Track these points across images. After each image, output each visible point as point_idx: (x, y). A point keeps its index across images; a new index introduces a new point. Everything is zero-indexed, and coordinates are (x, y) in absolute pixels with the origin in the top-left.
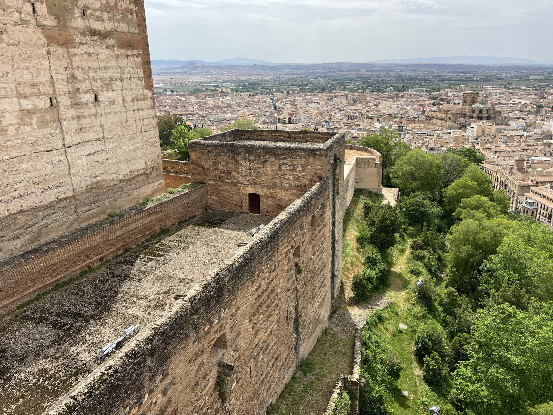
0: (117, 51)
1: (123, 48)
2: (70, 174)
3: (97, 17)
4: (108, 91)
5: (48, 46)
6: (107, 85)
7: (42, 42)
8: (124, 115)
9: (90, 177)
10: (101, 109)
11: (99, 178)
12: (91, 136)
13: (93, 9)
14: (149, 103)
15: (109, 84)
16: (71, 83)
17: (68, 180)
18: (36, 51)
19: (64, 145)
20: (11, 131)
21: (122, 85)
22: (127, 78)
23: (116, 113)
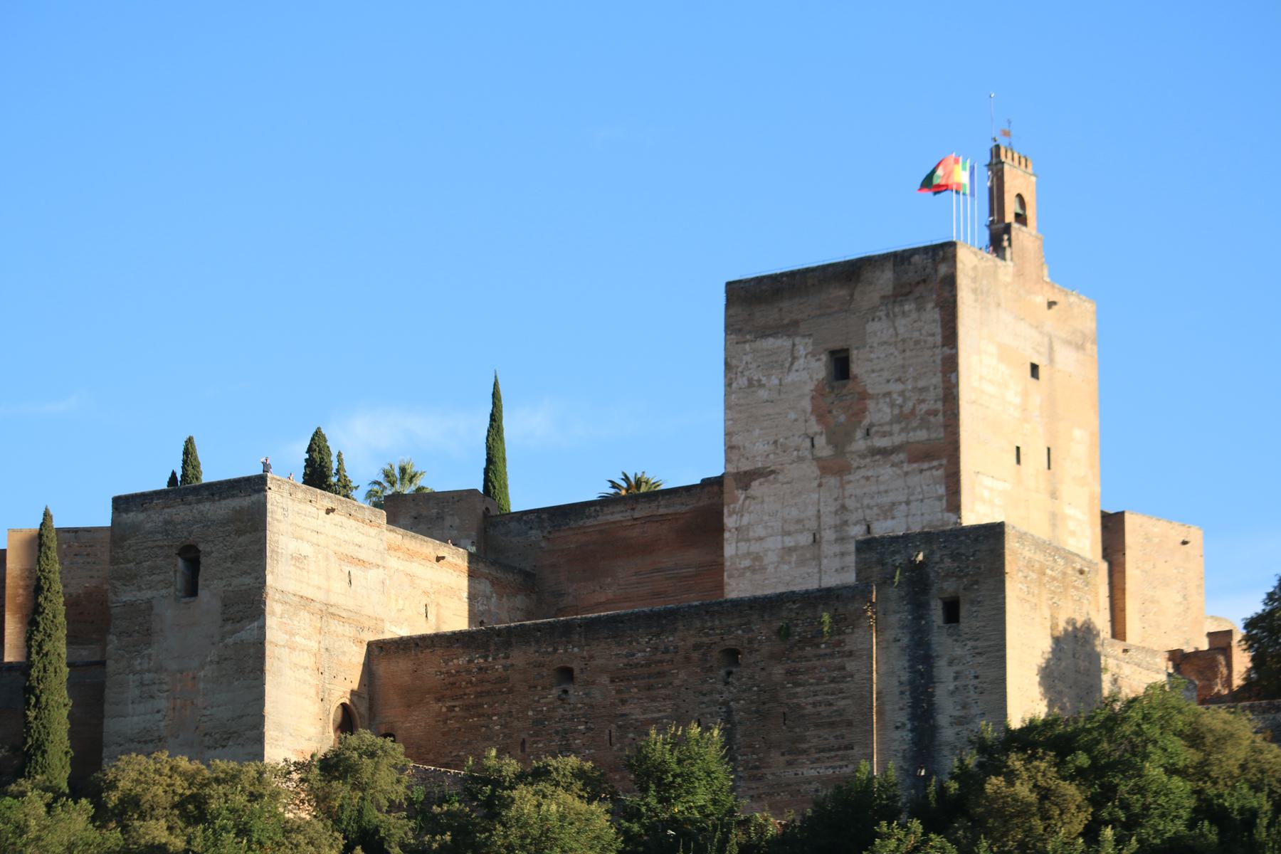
0: (906, 467)
1: (915, 462)
3: (885, 432)
4: (886, 519)
5: (821, 478)
7: (815, 475)
13: (881, 425)
20: (771, 569)
21: (909, 509)
22: (917, 500)
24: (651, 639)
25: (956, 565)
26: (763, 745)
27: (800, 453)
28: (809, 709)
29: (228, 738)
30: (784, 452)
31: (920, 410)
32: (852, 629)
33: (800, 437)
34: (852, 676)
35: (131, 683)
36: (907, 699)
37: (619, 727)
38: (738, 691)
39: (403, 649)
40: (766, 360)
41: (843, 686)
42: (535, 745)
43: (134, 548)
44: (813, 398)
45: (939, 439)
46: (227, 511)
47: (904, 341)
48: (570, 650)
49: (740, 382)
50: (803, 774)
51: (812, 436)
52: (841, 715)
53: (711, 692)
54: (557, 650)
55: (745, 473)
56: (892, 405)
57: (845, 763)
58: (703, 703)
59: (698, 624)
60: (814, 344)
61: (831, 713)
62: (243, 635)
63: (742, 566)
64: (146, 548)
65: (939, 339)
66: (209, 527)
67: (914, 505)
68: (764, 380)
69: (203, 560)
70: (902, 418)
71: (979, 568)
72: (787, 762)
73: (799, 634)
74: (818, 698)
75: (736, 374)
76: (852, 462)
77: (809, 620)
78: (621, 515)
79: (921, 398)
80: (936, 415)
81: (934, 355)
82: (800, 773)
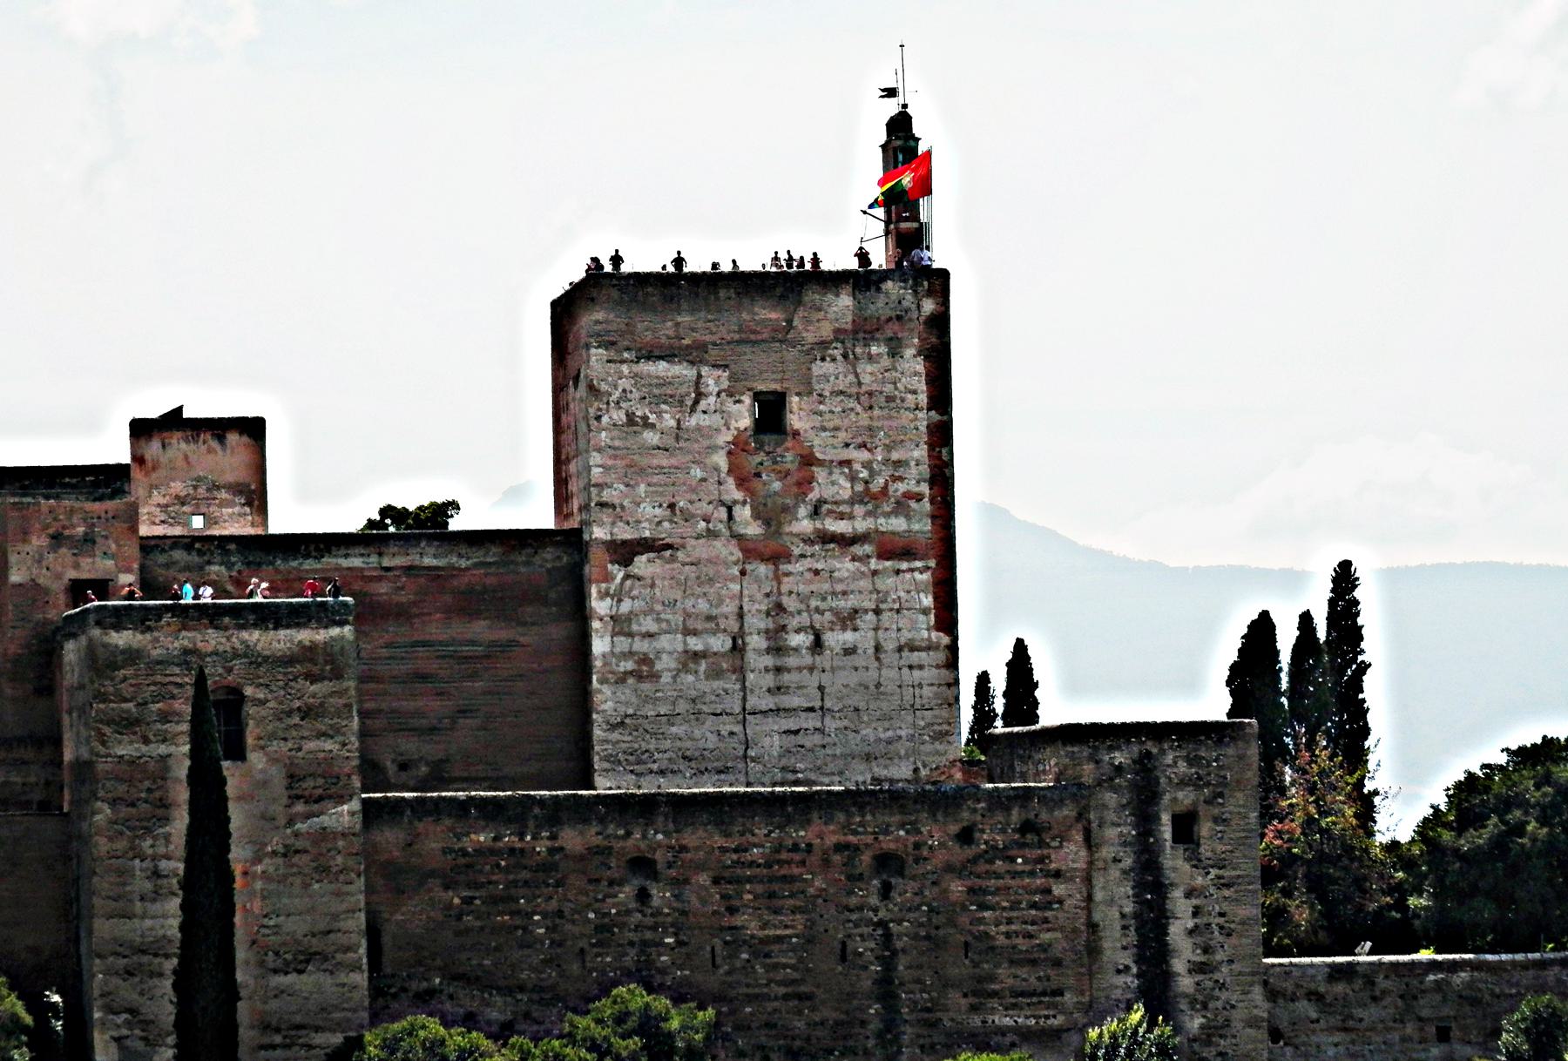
2: (745, 756)
4: (844, 629)
5: (744, 563)
7: (734, 558)
8: (873, 674)
9: (783, 769)
10: (824, 660)
11: (800, 775)
12: (795, 701)
13: (835, 503)
14: (941, 656)
15: (848, 620)
16: (773, 616)
17: (741, 766)
18: (723, 570)
19: (744, 709)
20: (666, 678)
21: (879, 620)
22: (891, 610)
23: (856, 669)
24: (770, 832)
25: (1193, 770)
26: (937, 982)
27: (711, 526)
28: (1001, 940)
29: (308, 962)
30: (686, 521)
31: (896, 490)
32: (1060, 842)
33: (710, 503)
34: (1060, 902)
35: (138, 873)
36: (1132, 937)
37: (726, 943)
38: (901, 910)
39: (389, 813)
40: (656, 391)
41: (1049, 914)
42: (599, 959)
43: (133, 682)
44: (730, 453)
45: (922, 532)
46: (288, 645)
47: (870, 394)
48: (649, 836)
49: (615, 417)
50: (993, 1021)
51: (730, 504)
52: (1045, 951)
53: (860, 908)
54: (632, 833)
55: (624, 542)
56: (853, 478)
57: (1051, 1013)
58: (850, 921)
59: (841, 817)
60: (730, 378)
61: (1033, 947)
62: (324, 820)
63: (622, 669)
64: (155, 684)
65: (923, 399)
66: (260, 665)
67: (885, 616)
68: (652, 418)
69: (250, 710)
71: (1225, 778)
72: (971, 1005)
73: (986, 843)
74: (1013, 927)
75: (608, 403)
77: (999, 826)
78: (361, 560)
79: (897, 474)
80: (919, 500)
81: (916, 419)
82: (990, 1021)
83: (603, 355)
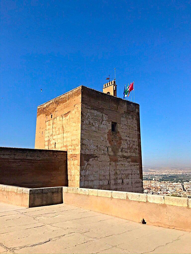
6: (126, 176)
7: (109, 160)
15: (127, 176)
44: (108, 135)
56: (127, 144)
70: (129, 148)
75: (85, 118)
76: (118, 159)
83: (84, 106)
